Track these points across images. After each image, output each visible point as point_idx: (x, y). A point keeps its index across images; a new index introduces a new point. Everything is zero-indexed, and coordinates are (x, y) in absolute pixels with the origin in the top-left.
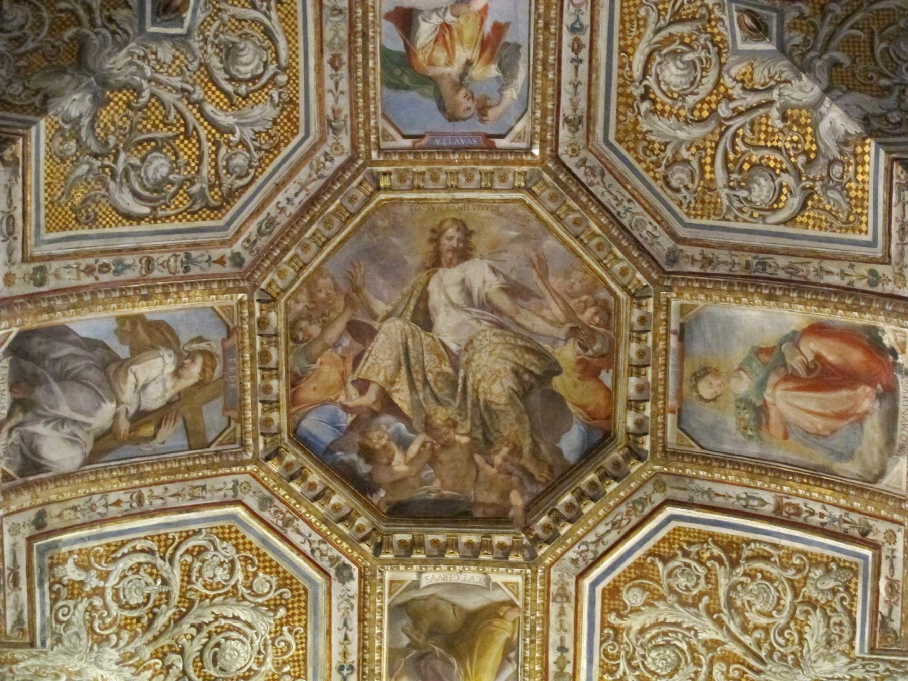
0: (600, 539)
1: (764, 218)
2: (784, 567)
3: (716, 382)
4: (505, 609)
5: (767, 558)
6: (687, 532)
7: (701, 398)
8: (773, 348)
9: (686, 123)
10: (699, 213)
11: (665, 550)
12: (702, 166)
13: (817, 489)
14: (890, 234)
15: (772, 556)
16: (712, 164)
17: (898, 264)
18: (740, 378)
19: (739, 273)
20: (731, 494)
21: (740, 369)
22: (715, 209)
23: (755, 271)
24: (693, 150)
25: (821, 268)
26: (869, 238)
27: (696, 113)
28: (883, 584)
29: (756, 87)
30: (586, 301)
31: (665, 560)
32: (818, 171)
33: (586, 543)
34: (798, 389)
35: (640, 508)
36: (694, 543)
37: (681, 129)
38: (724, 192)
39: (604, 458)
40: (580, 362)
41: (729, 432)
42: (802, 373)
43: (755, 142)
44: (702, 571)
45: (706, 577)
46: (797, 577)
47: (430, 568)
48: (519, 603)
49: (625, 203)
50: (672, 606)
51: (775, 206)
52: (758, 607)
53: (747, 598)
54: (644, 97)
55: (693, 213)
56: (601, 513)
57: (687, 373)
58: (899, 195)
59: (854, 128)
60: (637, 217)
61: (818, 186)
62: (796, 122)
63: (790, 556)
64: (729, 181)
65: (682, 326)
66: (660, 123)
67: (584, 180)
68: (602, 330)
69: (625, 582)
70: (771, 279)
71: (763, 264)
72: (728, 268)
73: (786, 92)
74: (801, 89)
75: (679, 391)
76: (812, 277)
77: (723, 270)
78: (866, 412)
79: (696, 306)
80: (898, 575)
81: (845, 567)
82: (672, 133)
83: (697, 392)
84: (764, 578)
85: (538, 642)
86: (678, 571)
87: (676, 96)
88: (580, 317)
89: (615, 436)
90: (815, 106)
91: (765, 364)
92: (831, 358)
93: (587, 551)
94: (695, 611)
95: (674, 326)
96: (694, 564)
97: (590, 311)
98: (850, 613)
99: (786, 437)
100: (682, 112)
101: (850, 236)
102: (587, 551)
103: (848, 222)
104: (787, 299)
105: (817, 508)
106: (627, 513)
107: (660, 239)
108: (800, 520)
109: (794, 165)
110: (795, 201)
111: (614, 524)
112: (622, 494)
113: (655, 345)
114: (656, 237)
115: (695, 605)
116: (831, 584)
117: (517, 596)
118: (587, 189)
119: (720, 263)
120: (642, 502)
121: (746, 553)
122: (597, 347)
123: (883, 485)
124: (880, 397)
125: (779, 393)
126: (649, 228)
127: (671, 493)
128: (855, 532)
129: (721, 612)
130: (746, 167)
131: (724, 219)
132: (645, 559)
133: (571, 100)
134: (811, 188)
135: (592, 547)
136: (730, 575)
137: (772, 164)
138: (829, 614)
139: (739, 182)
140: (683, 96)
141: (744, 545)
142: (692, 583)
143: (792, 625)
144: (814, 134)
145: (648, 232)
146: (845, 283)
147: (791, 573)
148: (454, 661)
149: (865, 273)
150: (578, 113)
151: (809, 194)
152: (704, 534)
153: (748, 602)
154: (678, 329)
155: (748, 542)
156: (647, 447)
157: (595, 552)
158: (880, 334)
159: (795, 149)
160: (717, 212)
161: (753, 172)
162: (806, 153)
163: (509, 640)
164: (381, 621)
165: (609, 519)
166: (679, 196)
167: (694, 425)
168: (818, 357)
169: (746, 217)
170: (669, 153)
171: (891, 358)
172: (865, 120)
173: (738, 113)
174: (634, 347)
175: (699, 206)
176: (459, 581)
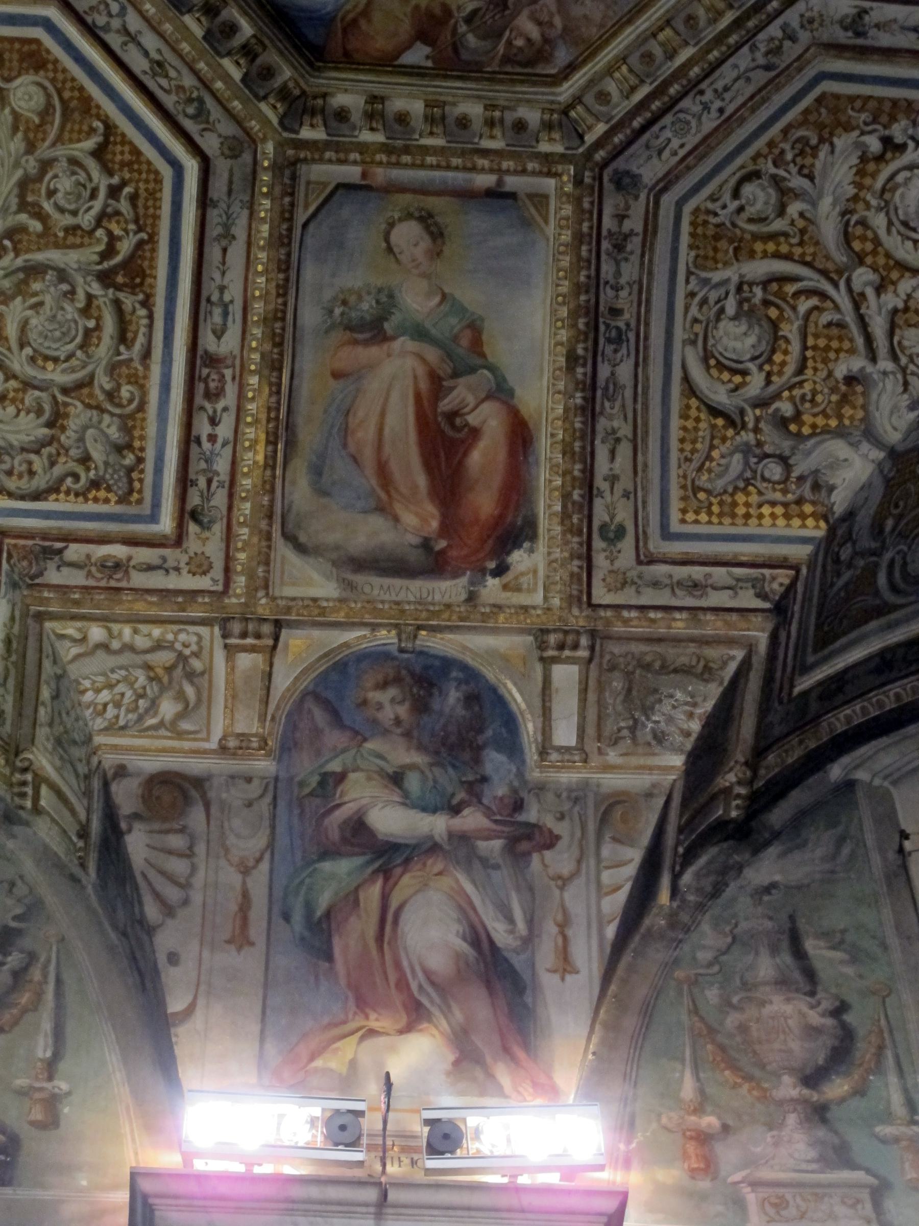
0: (132, 38)
1: (693, 343)
2: (113, 369)
3: (419, 252)
5: (123, 337)
6: (154, 195)
7: (391, 225)
8: (483, 355)
9: (843, 214)
10: (700, 230)
11: (119, 154)
12: (772, 237)
13: (263, 437)
14: (684, 563)
15: (128, 348)
16: (777, 255)
17: (640, 577)
18: (429, 295)
19: (602, 296)
20: (228, 276)
21: (444, 296)
22: (706, 258)
23: (607, 326)
24: (801, 223)
25: (618, 440)
26: (675, 527)
27: (859, 231)
28: (119, 551)
29: (898, 331)
30: (551, 24)
31: (98, 153)
32: (772, 439)
33: (123, 12)
34: (418, 397)
35: (191, 110)
37: (834, 204)
38: (731, 274)
39: (281, 53)
40: (447, 12)
41: (334, 275)
42: (446, 405)
43: (811, 329)
44: (86, 220)
45: (77, 227)
46: (97, 392)
49: (718, 104)
50: (17, 164)
51: (712, 362)
52: (34, 322)
53: (48, 299)
54: (887, 141)
55: (700, 220)
56: (185, 47)
57: (432, 202)
58: (747, 580)
59: (840, 501)
60: (694, 123)
61: (748, 437)
62: (845, 399)
64: (751, 284)
65: (513, 196)
66: (846, 167)
67: (761, 36)
68: (501, 49)
69: (53, 81)
71: (618, 339)
72: (610, 277)
73: (889, 383)
74: (895, 409)
76: (602, 424)
77: (607, 268)
78: (396, 519)
79: (546, 221)
80: (139, 580)
81: (131, 481)
82: (829, 187)
83: (400, 220)
84: (88, 333)
86: (82, 177)
87: (887, 196)
88: (525, 13)
89: (319, 69)
90: (870, 435)
91: (455, 338)
92: (476, 457)
93: (110, 15)
94: (14, 208)
95: (512, 182)
96: (98, 205)
97: (534, 32)
98: (54, 489)
99: (337, 375)
100: (860, 206)
101: (675, 493)
102: (110, 15)
103: (696, 489)
104: (571, 386)
105: (224, 430)
106: (180, 88)
107: (655, 160)
108: (199, 400)
109: (777, 396)
110: (720, 396)
111: (159, 64)
112: (219, 85)
113: (485, 153)
114: (660, 153)
115: (23, 206)
116: (98, 454)
118: (747, 41)
119: (618, 263)
120: (201, 114)
122: (472, 40)
123: (283, 550)
124: (426, 544)
125: (410, 362)
126: (675, 143)
127: (221, 167)
128: (194, 500)
129: (17, 256)
130: (773, 313)
131: (689, 273)
132: (98, 117)
133: (895, 21)
134: (744, 426)
135: (116, 23)
136: (84, 270)
137: (778, 358)
138: (45, 451)
139: (748, 300)
140: (886, 207)
141: (141, 297)
142: (62, 203)
143: (13, 384)
144: (826, 430)
145: (669, 140)
146: (600, 483)
147: (103, 381)
149: (618, 519)
150: (872, 32)
151: (734, 421)
152: (154, 225)
153: (41, 304)
154: (507, 188)
155: (147, 303)
156: (306, 133)
157: (107, 28)
158: (526, 545)
159: (803, 397)
160: (700, 261)
161: (764, 323)
162: (797, 417)
165: (169, 56)
166: (727, 197)
167: (346, 212)
168: (475, 433)
169: (694, 311)
170: (797, 182)
171: (492, 565)
172: (850, 515)
173: (858, 301)
174: (475, 110)
175: (711, 231)
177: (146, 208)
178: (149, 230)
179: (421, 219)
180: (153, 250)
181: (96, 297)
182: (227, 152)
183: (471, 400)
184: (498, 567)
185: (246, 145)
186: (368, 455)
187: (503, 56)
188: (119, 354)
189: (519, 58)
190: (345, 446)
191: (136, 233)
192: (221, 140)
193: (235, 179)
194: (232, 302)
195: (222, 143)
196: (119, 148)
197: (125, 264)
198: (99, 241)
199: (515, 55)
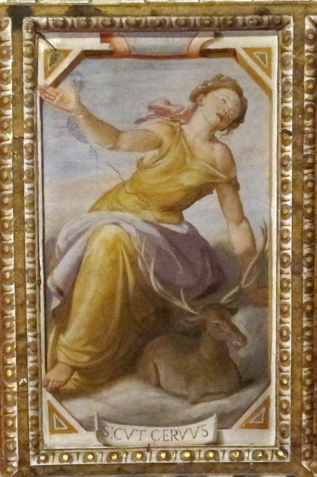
4: (70, 386)
47: (200, 457)
48: (47, 397)
85: (14, 335)
117: (52, 410)
148: (156, 285)
163: (62, 330)
164: (281, 361)
176: (150, 429)
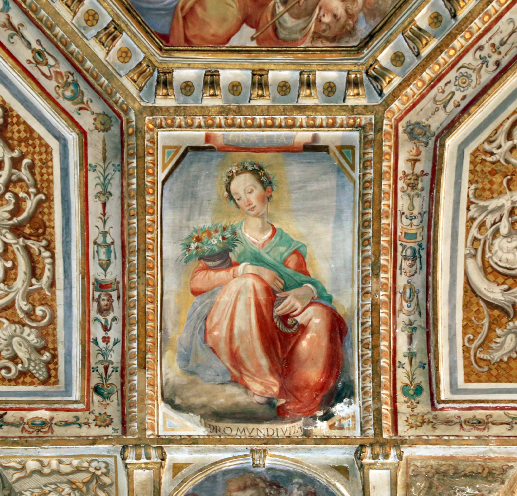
1: (474, 256)
3: (253, 198)
6: (46, 164)
7: (231, 178)
8: (306, 273)
10: (478, 168)
15: (38, 280)
18: (263, 231)
19: (399, 225)
20: (109, 224)
21: (274, 230)
23: (404, 247)
34: (258, 305)
35: (68, 93)
36: (33, 174)
41: (188, 220)
46: (19, 312)
51: (489, 270)
55: (478, 160)
57: (263, 158)
63: (44, 301)
65: (325, 149)
70: (395, 267)
75: (238, 148)
79: (353, 168)
83: (238, 173)
84: (7, 271)
91: (285, 263)
99: (196, 293)
108: (94, 313)
114: (445, 107)
121: (35, 246)
125: (250, 281)
126: (458, 96)
131: (470, 203)
141: (44, 243)
147: (22, 304)
152: (49, 188)
154: (321, 143)
166: (501, 138)
167: (194, 169)
169: (474, 232)
177: (42, 175)
178: (45, 191)
179: (254, 172)
180: (50, 207)
181: (11, 245)
182: (99, 126)
183: (299, 306)
184: (324, 414)
185: (113, 120)
186: (223, 347)
187: (314, 33)
188: (32, 285)
189: (325, 34)
190: (205, 341)
191: (35, 195)
192: (94, 116)
193: (107, 148)
194: (113, 243)
195: (95, 119)
196: (16, 128)
197: (31, 218)
198: (8, 202)
199: (324, 31)
